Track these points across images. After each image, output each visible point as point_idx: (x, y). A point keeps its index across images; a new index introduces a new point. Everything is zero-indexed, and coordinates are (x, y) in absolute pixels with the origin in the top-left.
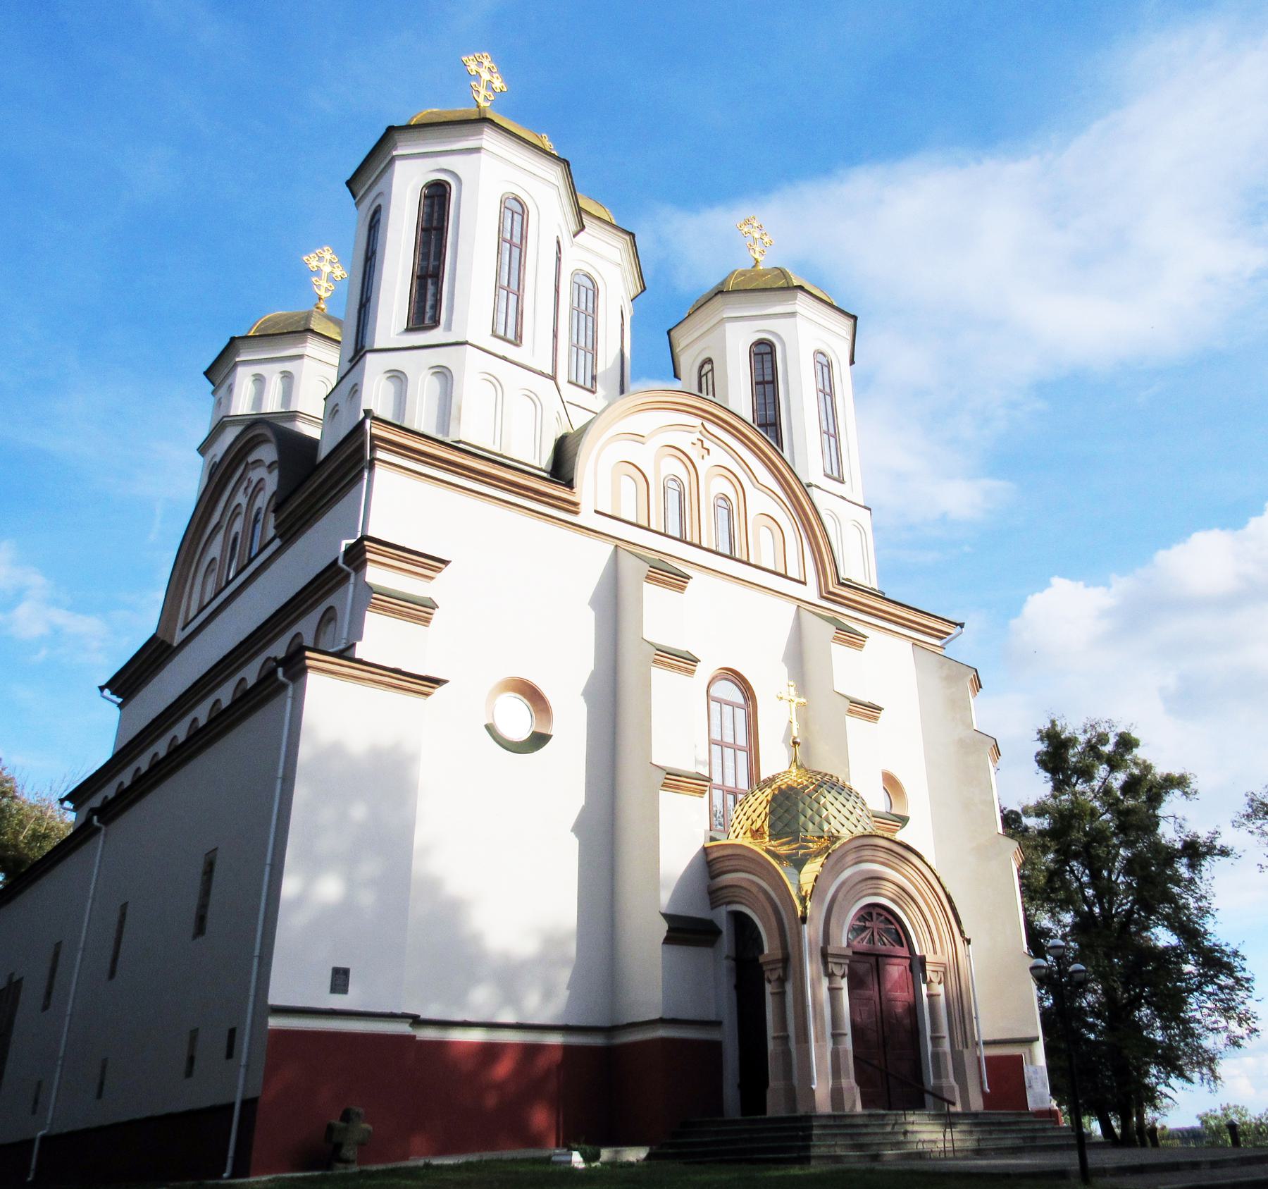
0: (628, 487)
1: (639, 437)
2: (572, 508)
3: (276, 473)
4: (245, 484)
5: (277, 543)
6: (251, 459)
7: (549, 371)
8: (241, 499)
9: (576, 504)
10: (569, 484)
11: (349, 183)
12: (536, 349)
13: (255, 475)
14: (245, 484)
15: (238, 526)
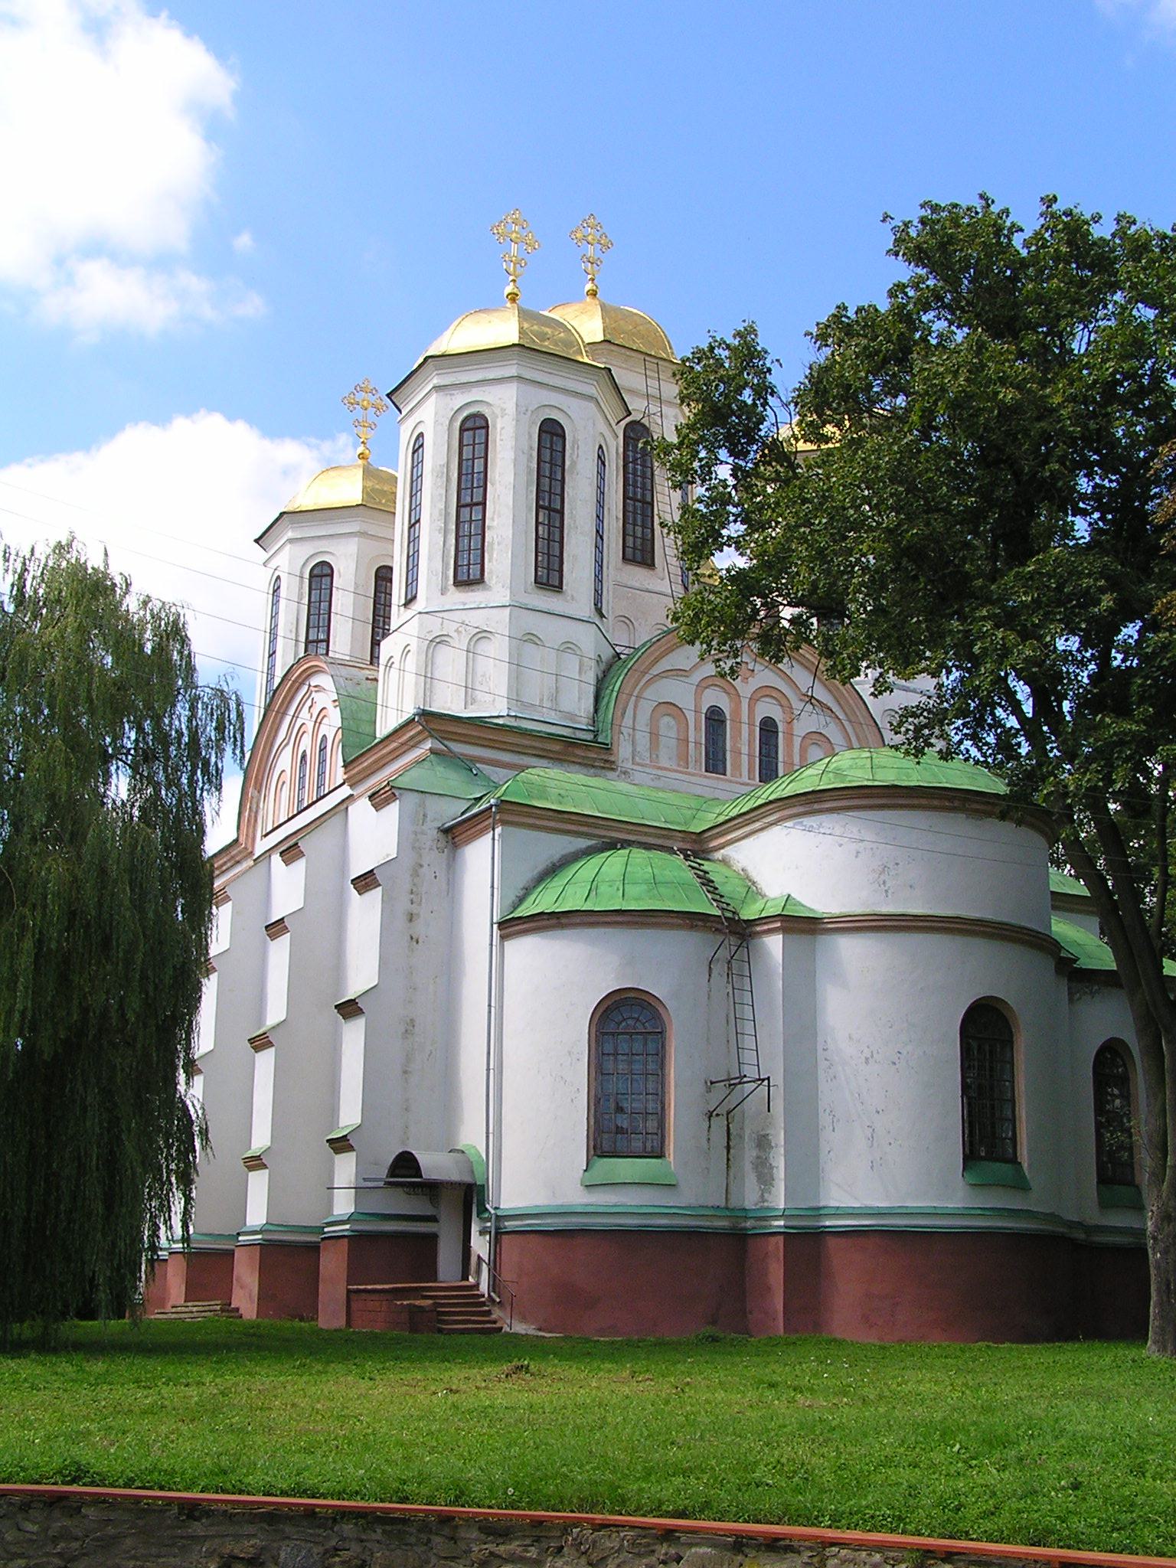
0: (668, 726)
4: (309, 703)
5: (346, 791)
6: (314, 681)
14: (309, 703)
15: (306, 744)
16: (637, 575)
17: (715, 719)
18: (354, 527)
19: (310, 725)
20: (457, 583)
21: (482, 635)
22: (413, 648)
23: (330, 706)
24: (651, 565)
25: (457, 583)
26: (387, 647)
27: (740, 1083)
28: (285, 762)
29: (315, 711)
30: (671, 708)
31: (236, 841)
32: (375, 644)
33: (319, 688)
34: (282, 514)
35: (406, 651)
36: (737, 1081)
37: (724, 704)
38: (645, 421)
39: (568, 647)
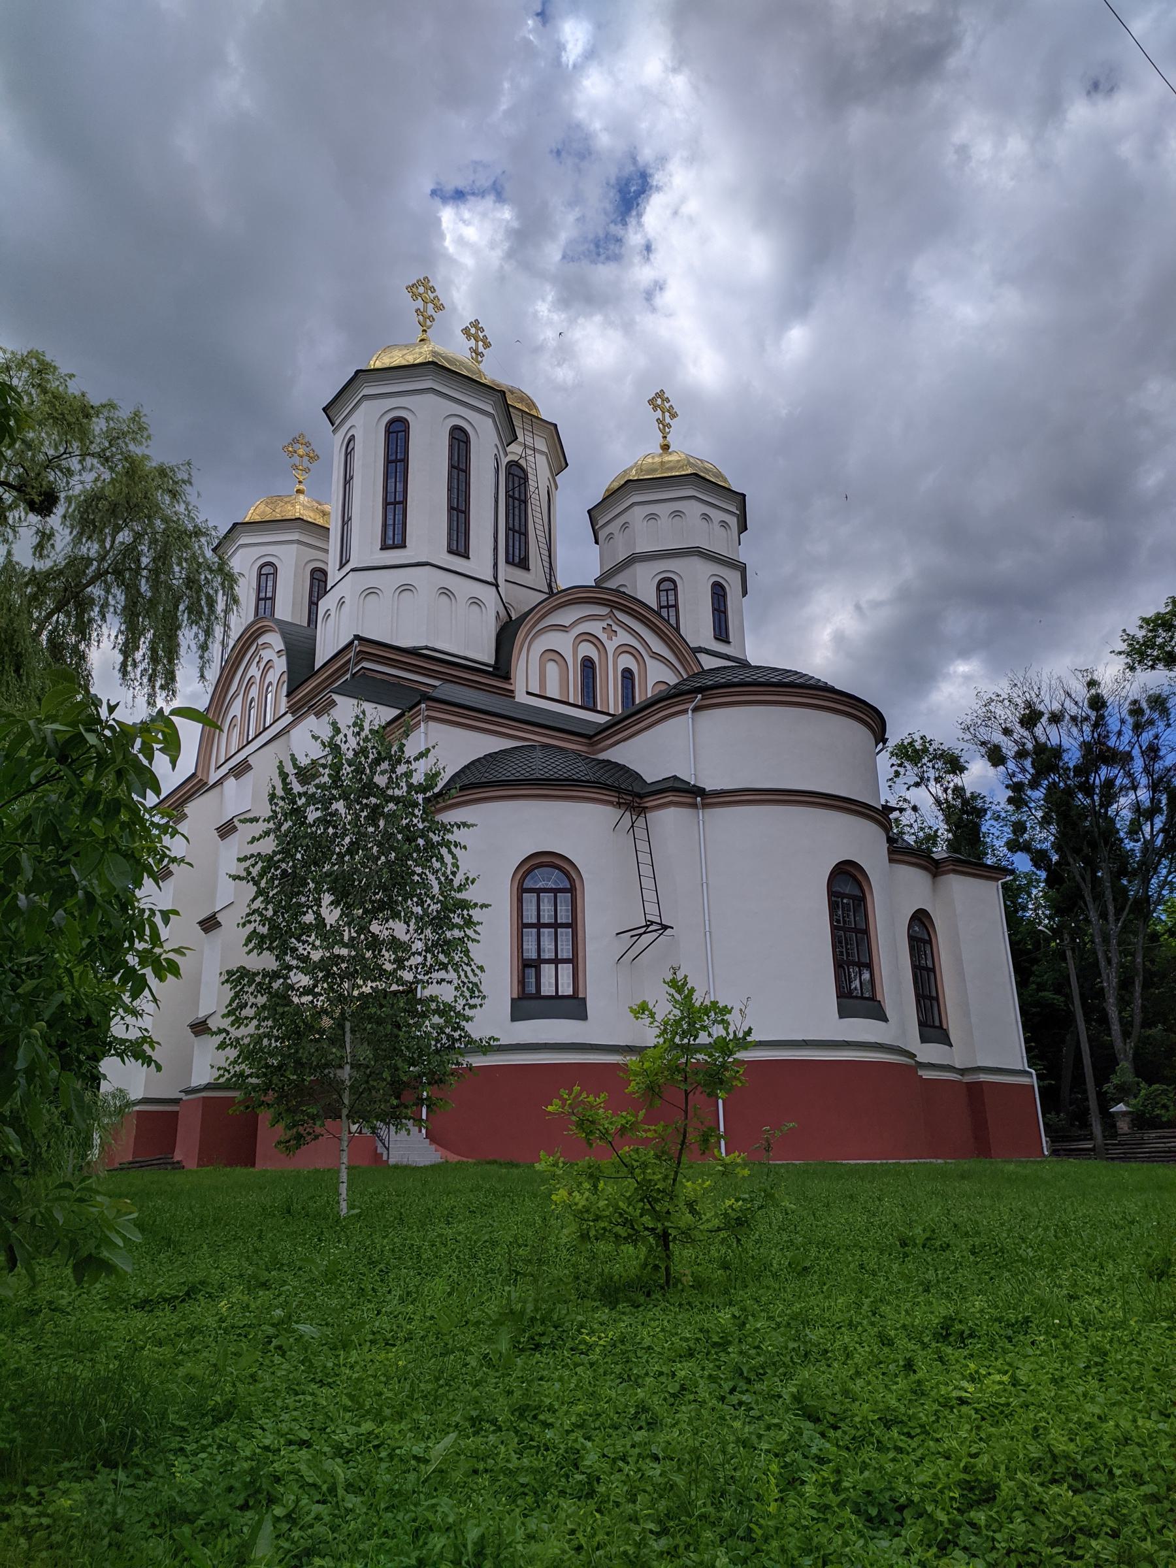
0: (552, 669)
1: (563, 628)
2: (510, 694)
3: (284, 658)
4: (257, 659)
5: (289, 718)
6: (261, 641)
7: (491, 579)
8: (254, 671)
9: (512, 691)
10: (507, 677)
11: (325, 409)
12: (481, 560)
13: (267, 654)
14: (257, 659)
15: (254, 692)
16: (518, 574)
17: (588, 665)
18: (295, 536)
19: (258, 676)
20: (384, 547)
21: (406, 588)
22: (347, 600)
23: (274, 657)
24: (528, 569)
25: (384, 547)
26: (324, 604)
27: (645, 933)
28: (236, 709)
29: (262, 665)
30: (553, 654)
31: (194, 775)
32: (313, 604)
33: (266, 645)
34: (235, 525)
35: (341, 602)
36: (643, 930)
37: (594, 654)
38: (522, 462)
39: (476, 602)
